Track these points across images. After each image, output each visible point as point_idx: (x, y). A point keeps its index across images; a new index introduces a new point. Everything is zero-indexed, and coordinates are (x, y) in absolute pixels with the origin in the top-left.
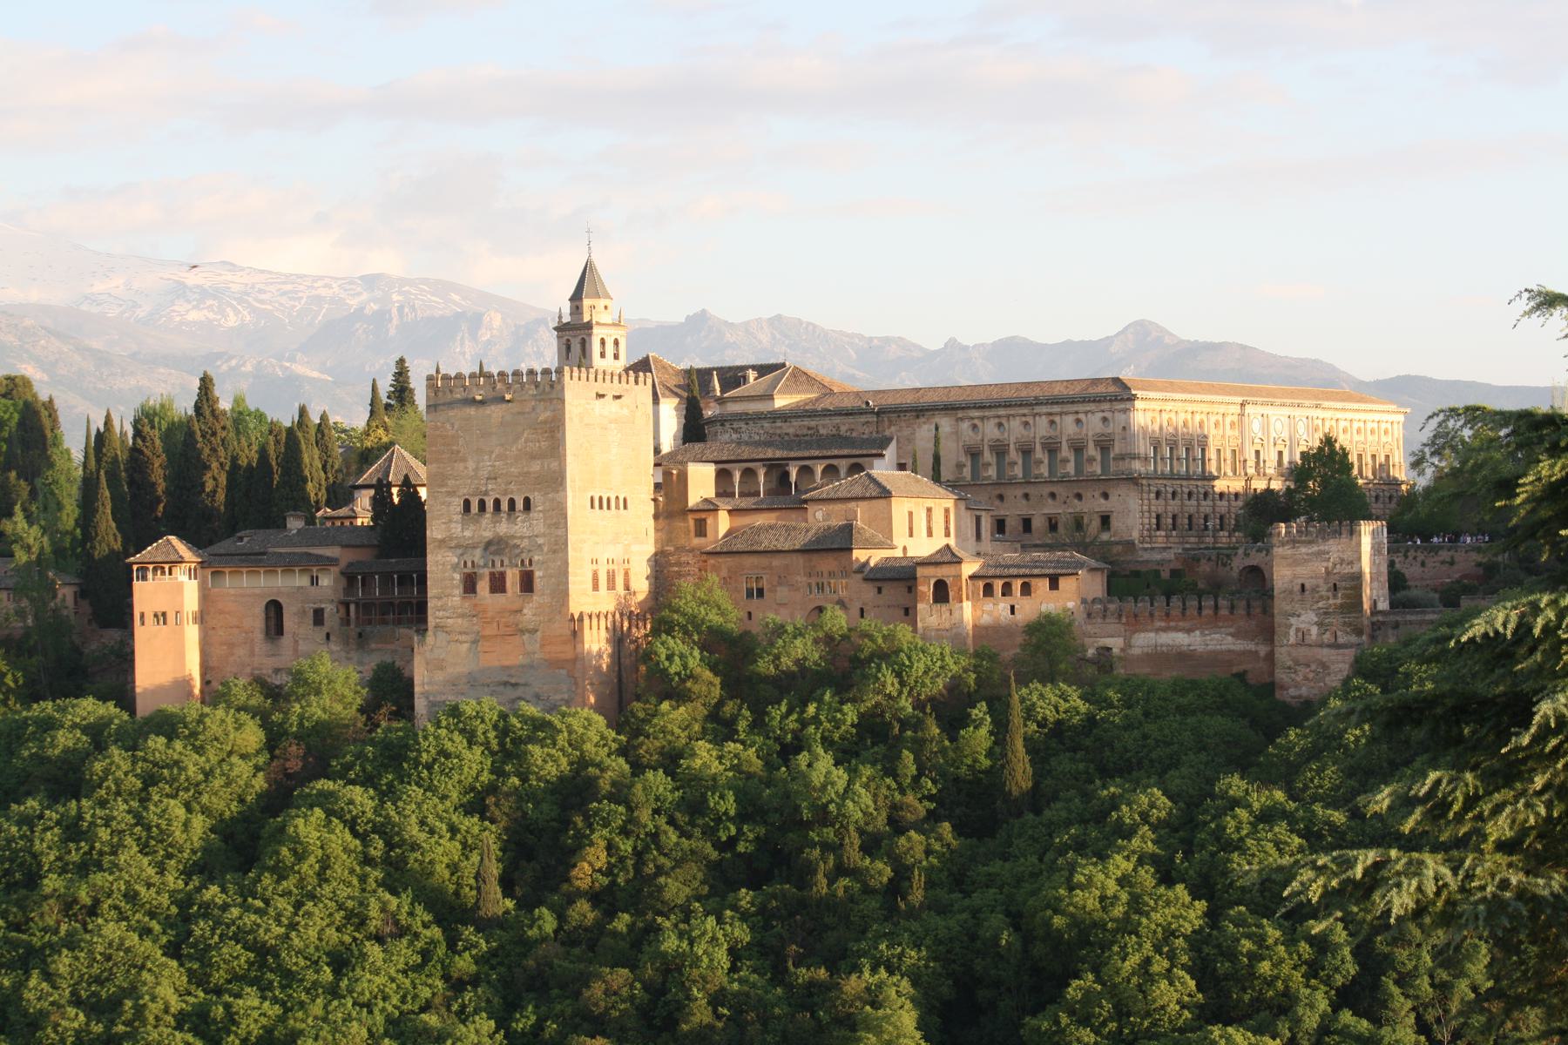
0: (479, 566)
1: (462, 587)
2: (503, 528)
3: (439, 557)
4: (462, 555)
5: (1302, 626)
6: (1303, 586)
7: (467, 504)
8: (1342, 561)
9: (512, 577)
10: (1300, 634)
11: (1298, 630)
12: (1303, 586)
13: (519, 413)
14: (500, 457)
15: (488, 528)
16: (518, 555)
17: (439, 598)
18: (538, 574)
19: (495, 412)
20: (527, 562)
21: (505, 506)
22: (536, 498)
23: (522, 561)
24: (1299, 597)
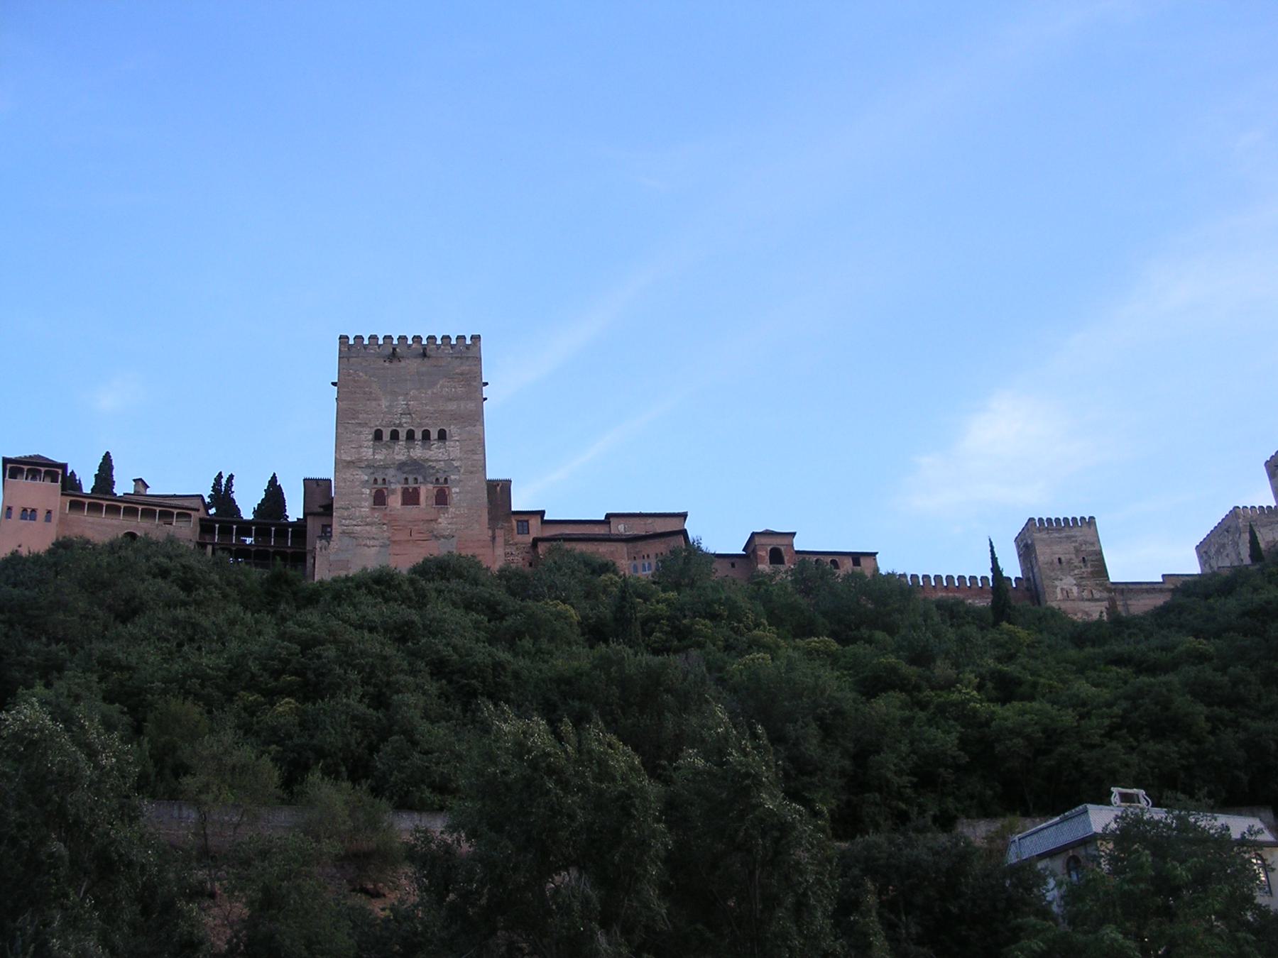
0: (390, 483)
1: (371, 500)
2: (418, 452)
3: (348, 475)
4: (373, 473)
5: (1065, 587)
6: (1059, 559)
7: (378, 436)
8: (1086, 543)
9: (426, 491)
10: (1065, 592)
11: (1062, 589)
12: (1059, 559)
13: (435, 366)
14: (415, 398)
15: (400, 452)
16: (433, 475)
17: (348, 508)
18: (454, 490)
19: (413, 365)
20: (442, 480)
21: (418, 435)
22: (452, 430)
23: (437, 479)
24: (1059, 567)
